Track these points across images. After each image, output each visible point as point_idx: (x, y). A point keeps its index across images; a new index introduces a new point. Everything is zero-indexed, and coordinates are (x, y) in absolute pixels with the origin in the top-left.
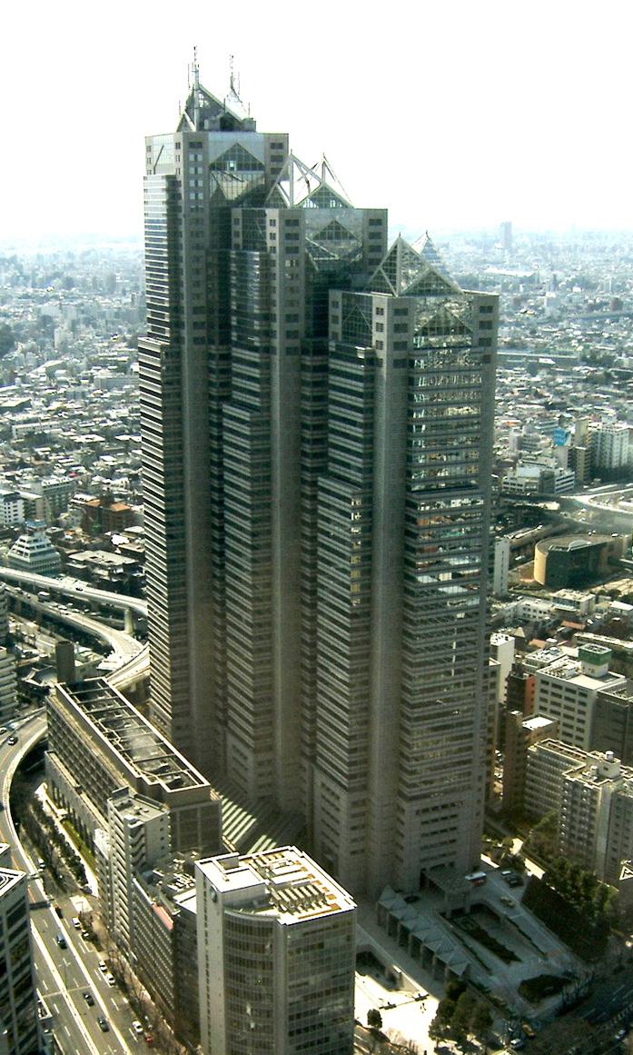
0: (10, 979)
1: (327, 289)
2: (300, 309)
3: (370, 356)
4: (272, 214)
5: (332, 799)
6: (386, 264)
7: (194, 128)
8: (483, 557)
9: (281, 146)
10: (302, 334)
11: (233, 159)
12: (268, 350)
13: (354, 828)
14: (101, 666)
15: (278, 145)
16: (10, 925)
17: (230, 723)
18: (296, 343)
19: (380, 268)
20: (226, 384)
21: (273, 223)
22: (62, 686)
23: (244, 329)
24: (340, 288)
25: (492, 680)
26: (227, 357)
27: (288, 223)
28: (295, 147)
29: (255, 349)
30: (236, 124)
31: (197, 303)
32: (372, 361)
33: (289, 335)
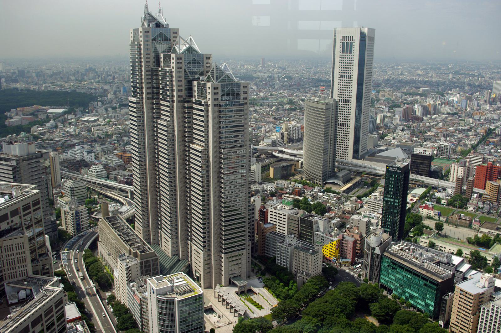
0: (56, 328)
1: (192, 81)
2: (184, 88)
3: (206, 103)
4: (173, 55)
5: (198, 254)
6: (211, 72)
7: (146, 26)
8: (246, 170)
9: (176, 33)
10: (184, 96)
11: (160, 37)
12: (173, 101)
13: (206, 264)
14: (119, 211)
15: (176, 32)
16: (56, 308)
17: (163, 230)
18: (182, 99)
19: (209, 74)
20: (159, 113)
21: (173, 59)
22: (104, 218)
23: (164, 94)
24: (196, 80)
25: (252, 212)
26: (158, 104)
27: (178, 59)
28: (181, 33)
29: (168, 101)
30: (161, 25)
31: (148, 86)
32: (207, 105)
33: (179, 96)
